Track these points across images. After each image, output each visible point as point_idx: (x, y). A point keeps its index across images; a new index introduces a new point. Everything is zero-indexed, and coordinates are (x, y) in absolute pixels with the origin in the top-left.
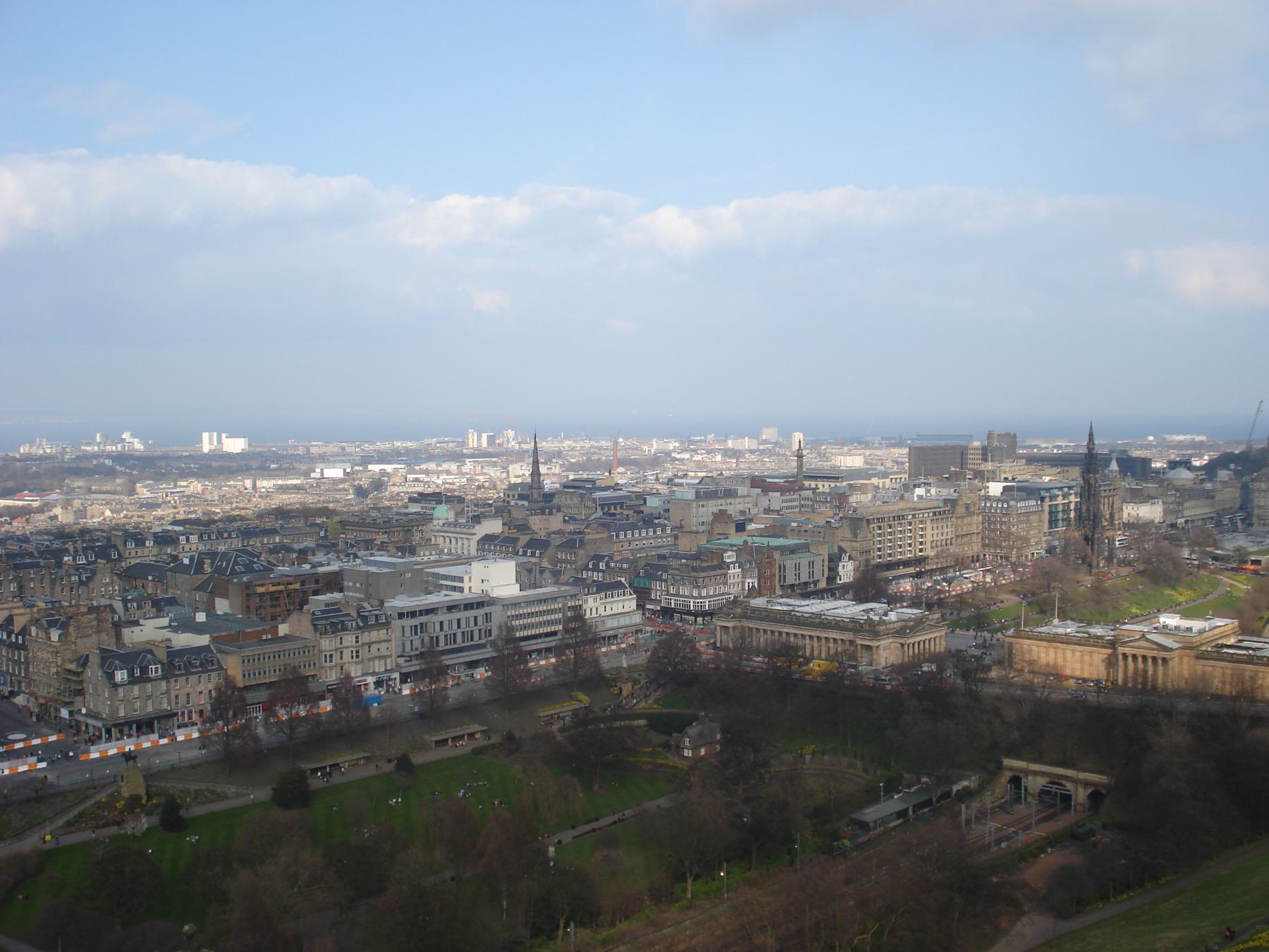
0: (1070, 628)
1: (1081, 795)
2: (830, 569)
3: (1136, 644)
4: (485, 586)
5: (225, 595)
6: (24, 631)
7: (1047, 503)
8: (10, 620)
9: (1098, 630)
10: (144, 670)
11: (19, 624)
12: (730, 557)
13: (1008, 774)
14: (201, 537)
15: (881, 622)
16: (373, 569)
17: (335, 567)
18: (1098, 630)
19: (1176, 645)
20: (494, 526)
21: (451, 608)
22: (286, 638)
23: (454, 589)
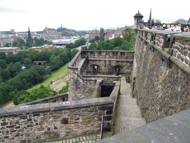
0: (35, 47)
1: (43, 64)
9: (38, 47)
18: (38, 47)
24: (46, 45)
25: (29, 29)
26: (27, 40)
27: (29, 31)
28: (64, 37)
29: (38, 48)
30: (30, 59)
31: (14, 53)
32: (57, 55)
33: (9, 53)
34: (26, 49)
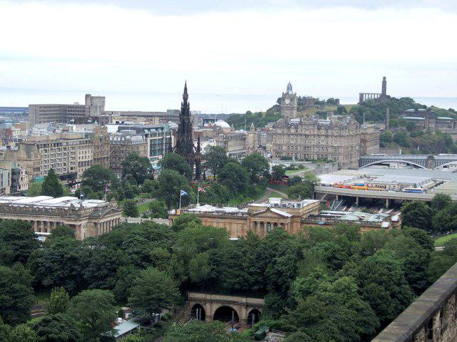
0: (207, 208)
1: (243, 314)
2: (13, 180)
3: (264, 215)
7: (149, 139)
9: (228, 209)
13: (192, 304)
15: (82, 208)
18: (228, 209)
19: (289, 215)
24: (275, 201)
25: (185, 96)
26: (167, 164)
27: (185, 106)
28: (397, 157)
29: (224, 216)
30: (168, 279)
31: (84, 232)
32: (338, 267)
33: (55, 233)
34: (157, 212)
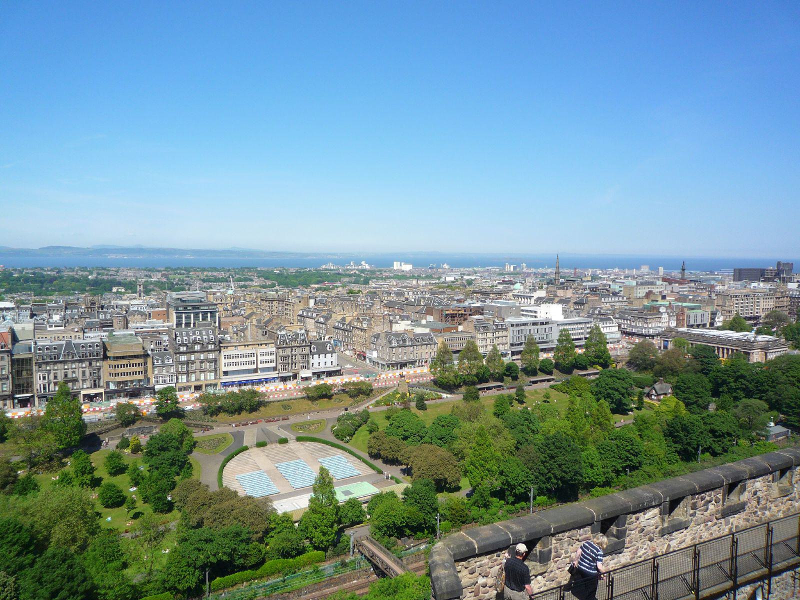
4: (547, 316)
5: (431, 315)
6: (350, 324)
8: (344, 319)
10: (404, 341)
11: (348, 321)
12: (662, 310)
14: (414, 293)
16: (499, 305)
17: (479, 304)
20: (542, 293)
21: (534, 324)
22: (462, 331)
23: (532, 316)
